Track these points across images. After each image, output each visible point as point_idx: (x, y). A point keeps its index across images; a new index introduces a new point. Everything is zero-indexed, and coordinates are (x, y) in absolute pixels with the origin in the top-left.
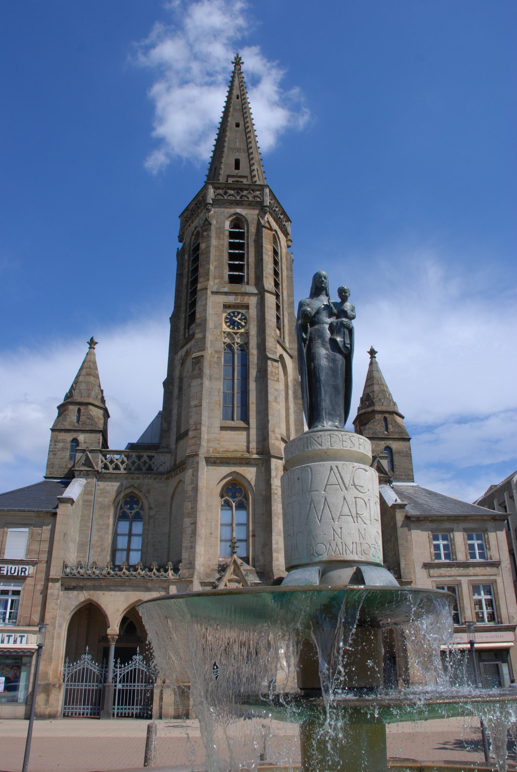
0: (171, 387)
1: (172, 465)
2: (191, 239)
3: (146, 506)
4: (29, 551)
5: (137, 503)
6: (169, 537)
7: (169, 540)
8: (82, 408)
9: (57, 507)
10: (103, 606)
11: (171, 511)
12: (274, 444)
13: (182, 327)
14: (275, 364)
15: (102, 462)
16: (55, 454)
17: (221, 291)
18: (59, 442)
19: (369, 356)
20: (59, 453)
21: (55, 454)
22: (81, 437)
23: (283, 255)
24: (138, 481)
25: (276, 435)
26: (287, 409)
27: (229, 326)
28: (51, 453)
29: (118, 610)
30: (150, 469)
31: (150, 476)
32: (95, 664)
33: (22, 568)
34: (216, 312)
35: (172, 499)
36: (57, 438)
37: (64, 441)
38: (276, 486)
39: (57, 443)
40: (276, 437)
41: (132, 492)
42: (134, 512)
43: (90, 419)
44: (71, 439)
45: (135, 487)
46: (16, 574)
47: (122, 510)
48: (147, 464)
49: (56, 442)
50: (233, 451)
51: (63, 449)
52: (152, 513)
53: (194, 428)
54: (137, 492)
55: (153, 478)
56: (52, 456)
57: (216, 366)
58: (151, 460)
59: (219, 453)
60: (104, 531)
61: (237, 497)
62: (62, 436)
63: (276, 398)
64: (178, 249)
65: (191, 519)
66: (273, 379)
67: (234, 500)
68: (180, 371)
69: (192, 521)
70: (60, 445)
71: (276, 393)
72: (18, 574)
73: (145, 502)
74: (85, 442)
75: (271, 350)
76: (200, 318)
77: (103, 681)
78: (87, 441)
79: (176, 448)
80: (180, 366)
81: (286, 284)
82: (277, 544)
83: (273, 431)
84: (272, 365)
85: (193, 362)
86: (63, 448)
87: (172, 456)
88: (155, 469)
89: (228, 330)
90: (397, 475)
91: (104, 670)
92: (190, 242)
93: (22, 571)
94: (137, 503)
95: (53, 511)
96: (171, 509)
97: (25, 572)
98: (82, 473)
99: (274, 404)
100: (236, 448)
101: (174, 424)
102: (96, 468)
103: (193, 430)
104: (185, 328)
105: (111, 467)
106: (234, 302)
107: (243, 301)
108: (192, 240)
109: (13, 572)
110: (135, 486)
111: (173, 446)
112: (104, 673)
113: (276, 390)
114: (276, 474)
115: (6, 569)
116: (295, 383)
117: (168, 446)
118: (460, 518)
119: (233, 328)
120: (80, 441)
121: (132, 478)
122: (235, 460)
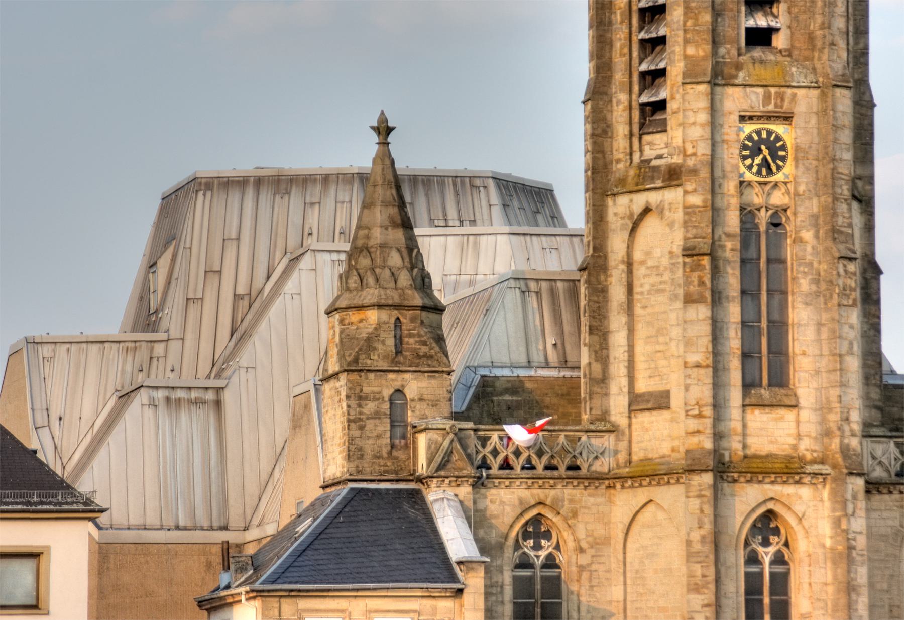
0: (602, 278)
5: (548, 535)
11: (625, 558)
18: (366, 398)
20: (370, 424)
21: (362, 428)
24: (552, 493)
28: (352, 425)
30: (574, 467)
31: (575, 482)
36: (361, 391)
37: (377, 398)
38: (854, 532)
39: (364, 403)
40: (852, 430)
41: (539, 514)
42: (543, 554)
43: (424, 343)
44: (392, 391)
47: (521, 551)
51: (377, 415)
52: (584, 560)
53: (696, 412)
56: (357, 433)
62: (372, 385)
65: (702, 597)
68: (628, 247)
69: (706, 602)
73: (567, 535)
75: (841, 232)
76: (694, 154)
78: (425, 397)
79: (630, 425)
84: (846, 271)
85: (685, 264)
94: (548, 535)
96: (625, 553)
98: (447, 481)
103: (695, 416)
105: (495, 463)
106: (762, 108)
107: (782, 107)
110: (548, 502)
114: (854, 509)
116: (866, 265)
117: (604, 416)
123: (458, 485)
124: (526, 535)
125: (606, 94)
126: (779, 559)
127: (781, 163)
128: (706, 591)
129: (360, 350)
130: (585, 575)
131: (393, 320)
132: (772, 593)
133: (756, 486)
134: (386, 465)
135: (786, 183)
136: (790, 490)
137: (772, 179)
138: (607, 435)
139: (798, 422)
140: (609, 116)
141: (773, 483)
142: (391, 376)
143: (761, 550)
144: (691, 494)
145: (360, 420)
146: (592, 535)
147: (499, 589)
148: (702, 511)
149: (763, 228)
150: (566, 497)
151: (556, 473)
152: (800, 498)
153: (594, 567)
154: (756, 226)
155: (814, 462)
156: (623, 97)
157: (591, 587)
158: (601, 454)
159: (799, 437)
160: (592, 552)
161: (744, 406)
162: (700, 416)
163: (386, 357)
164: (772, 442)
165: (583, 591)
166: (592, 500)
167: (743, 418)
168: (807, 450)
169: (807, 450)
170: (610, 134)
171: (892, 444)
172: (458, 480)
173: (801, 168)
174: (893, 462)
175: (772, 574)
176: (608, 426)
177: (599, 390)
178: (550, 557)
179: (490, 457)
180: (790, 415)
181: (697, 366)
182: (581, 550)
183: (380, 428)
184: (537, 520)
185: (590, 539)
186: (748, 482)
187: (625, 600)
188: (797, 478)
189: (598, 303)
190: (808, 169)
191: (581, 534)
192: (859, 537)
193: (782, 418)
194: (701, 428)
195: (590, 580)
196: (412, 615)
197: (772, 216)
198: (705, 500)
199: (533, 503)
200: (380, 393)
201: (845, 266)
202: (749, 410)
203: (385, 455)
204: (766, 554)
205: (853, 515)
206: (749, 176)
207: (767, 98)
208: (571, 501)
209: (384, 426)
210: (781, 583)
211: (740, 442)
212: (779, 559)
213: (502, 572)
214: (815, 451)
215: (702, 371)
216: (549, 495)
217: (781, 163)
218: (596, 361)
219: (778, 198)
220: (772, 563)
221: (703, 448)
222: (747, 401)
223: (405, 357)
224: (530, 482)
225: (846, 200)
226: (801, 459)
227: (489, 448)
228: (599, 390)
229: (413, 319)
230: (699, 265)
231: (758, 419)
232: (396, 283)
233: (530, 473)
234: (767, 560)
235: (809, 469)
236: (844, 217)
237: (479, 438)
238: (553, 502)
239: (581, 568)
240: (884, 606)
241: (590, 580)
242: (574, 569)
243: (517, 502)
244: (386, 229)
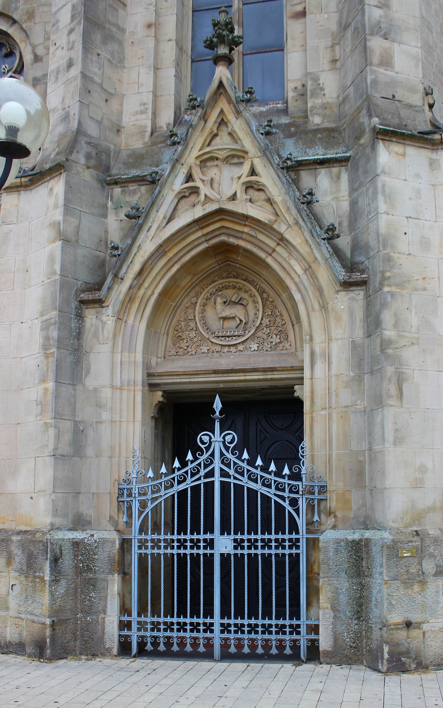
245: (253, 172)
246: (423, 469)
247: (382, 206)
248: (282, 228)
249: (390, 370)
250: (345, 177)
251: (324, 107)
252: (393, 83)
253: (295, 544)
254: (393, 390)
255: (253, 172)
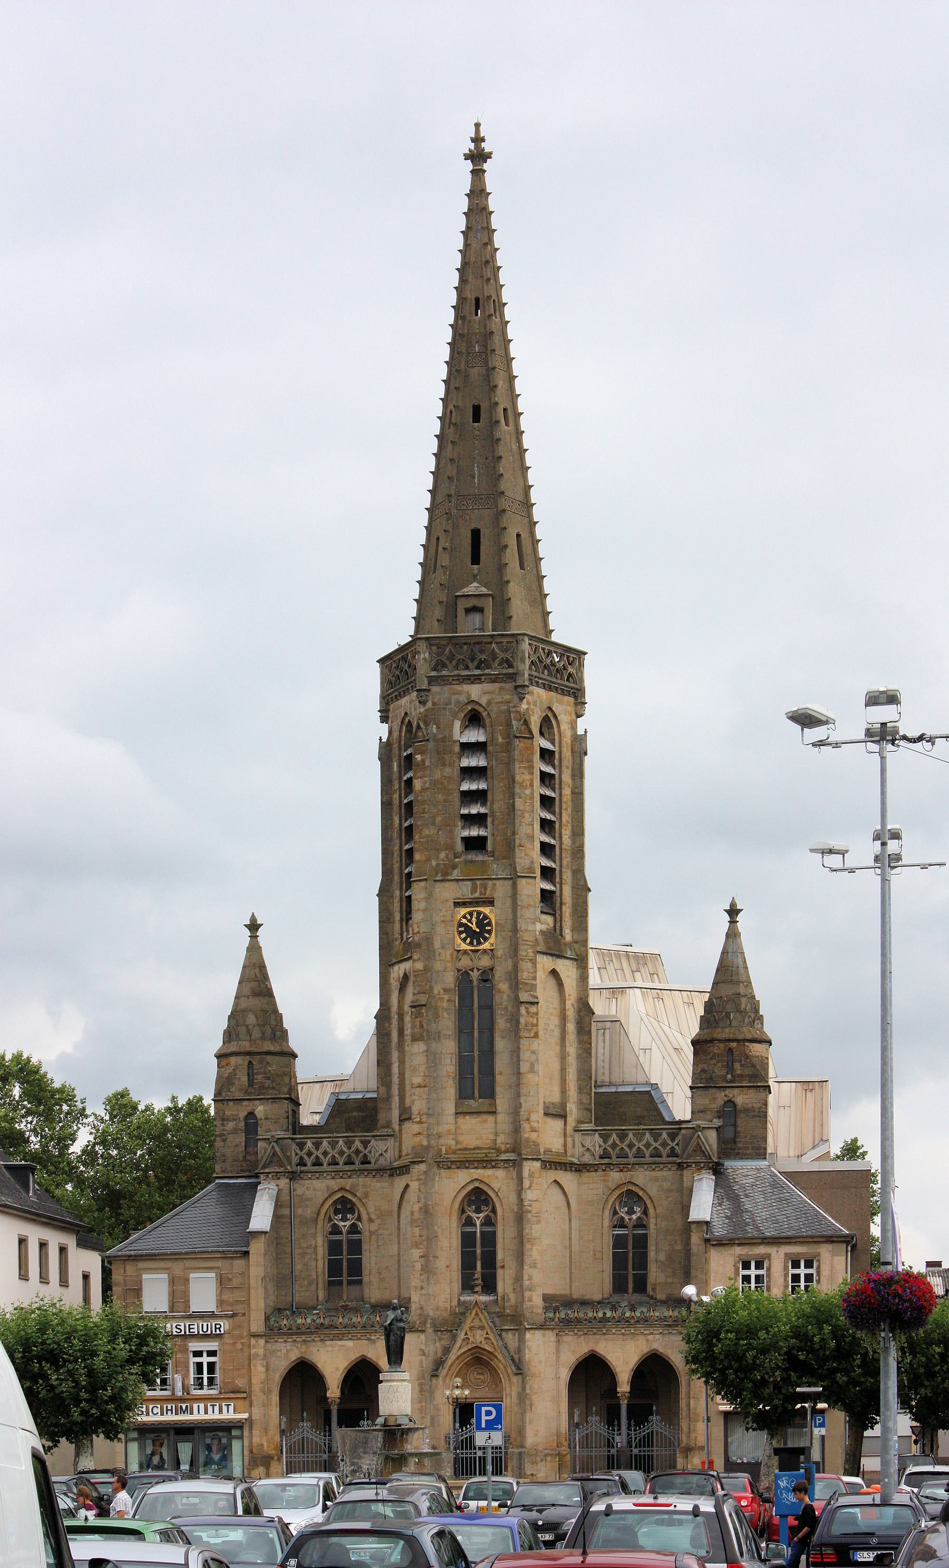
0: (387, 1025)
1: (397, 1156)
2: (400, 731)
3: (364, 1216)
4: (220, 1302)
6: (399, 1261)
7: (399, 1266)
8: (256, 1060)
9: (247, 1245)
10: (319, 1365)
11: (399, 1225)
12: (528, 1138)
13: (397, 916)
14: (533, 1009)
15: (297, 1154)
16: (224, 1141)
17: (450, 878)
18: (228, 1120)
19: (727, 918)
20: (230, 1138)
21: (224, 1141)
22: (260, 1110)
23: (564, 742)
25: (532, 1124)
26: (563, 1057)
27: (464, 940)
29: (337, 1369)
30: (366, 1161)
31: (366, 1173)
32: (316, 1432)
33: (216, 1325)
34: (442, 919)
35: (400, 1207)
36: (224, 1114)
38: (530, 1201)
40: (531, 1127)
41: (343, 1196)
42: (348, 1223)
43: (268, 1078)
44: (245, 1113)
45: (347, 1190)
46: (209, 1332)
47: (332, 1223)
48: (361, 1155)
49: (223, 1120)
50: (475, 1149)
51: (235, 1131)
52: (373, 1227)
54: (350, 1197)
55: (371, 1176)
57: (445, 1015)
58: (365, 1148)
59: (454, 1153)
60: (309, 1256)
61: (480, 1212)
63: (532, 1066)
64: (381, 739)
66: (527, 1035)
67: (478, 1215)
70: (231, 1125)
71: (533, 1058)
72: (212, 1332)
74: (266, 1119)
75: (527, 984)
77: (327, 1450)
78: (269, 1117)
79: (400, 1131)
80: (397, 991)
81: (570, 810)
82: (530, 1279)
83: (528, 1120)
84: (528, 1012)
86: (235, 1129)
87: (395, 1142)
88: (373, 1161)
89: (464, 946)
90: (740, 1149)
91: (327, 1438)
92: (400, 736)
93: (216, 1328)
95: (244, 1249)
96: (399, 1222)
97: (219, 1329)
98: (270, 1176)
99: (530, 1076)
100: (478, 1143)
101: (395, 1090)
102: (289, 1167)
104: (401, 918)
108: (403, 734)
109: (205, 1330)
110: (348, 1188)
111: (397, 1128)
112: (327, 1442)
113: (533, 1052)
114: (531, 1184)
115: (195, 1327)
117: (388, 1125)
118: (781, 1241)
119: (471, 943)
120: (259, 1116)
121: (341, 1178)
122: (476, 1163)
123: (279, 1178)
124: (337, 1212)
125: (388, 891)
126: (488, 1222)
127: (487, 936)
128: (422, 1246)
129: (223, 1085)
130: (374, 1237)
131: (246, 1063)
132: (482, 1246)
133: (464, 1170)
134: (242, 1166)
135: (492, 950)
136: (489, 1172)
137: (480, 947)
138: (389, 1138)
139: (496, 1123)
140: (391, 907)
141: (476, 1168)
142: (245, 1103)
143: (474, 1215)
144: (414, 1178)
145: (224, 1135)
146: (379, 1210)
147: (313, 1250)
148: (420, 1190)
149: (475, 983)
150: (361, 1183)
151: (352, 1167)
152: (497, 1178)
153: (381, 1231)
154: (471, 981)
155: (507, 1151)
156: (397, 893)
157: (378, 1246)
158: (385, 1152)
159: (496, 1134)
160: (378, 1221)
161: (456, 1113)
162: (420, 1122)
163: (241, 1090)
164: (477, 1139)
165: (372, 1249)
166: (379, 1185)
167: (456, 1122)
168: (502, 1143)
169: (502, 1143)
170: (392, 920)
171: (597, 1135)
172: (277, 1176)
173: (500, 939)
174: (597, 1148)
175: (482, 1233)
176: (390, 1131)
177: (384, 1106)
178: (354, 1226)
179: (305, 1157)
180: (491, 1118)
181: (419, 1087)
182: (371, 1220)
183: (238, 1140)
184: (343, 1200)
185: (378, 1212)
186: (458, 1168)
187: (399, 1254)
188: (493, 1164)
189: (383, 1043)
190: (504, 939)
191: (371, 1210)
192: (534, 1204)
193: (485, 1121)
194: (421, 1131)
195: (377, 1242)
196: (216, 1270)
197: (482, 974)
198: (422, 1182)
199: (337, 1189)
200: (236, 1115)
201: (527, 1008)
202: (461, 1117)
203: (241, 1159)
204: (478, 1218)
205: (530, 1188)
206: (464, 946)
207: (474, 890)
208: (364, 1186)
209: (241, 1138)
210: (490, 1239)
211: (453, 1139)
212: (488, 1222)
213: (315, 1238)
214: (507, 1144)
215: (422, 1090)
216: (348, 1183)
217: (487, 936)
218: (383, 1085)
219: (485, 962)
220: (482, 1225)
221: (422, 1146)
222: (459, 1111)
223: (255, 1089)
224: (333, 1174)
225: (530, 960)
226: (499, 1151)
227: (321, 1150)
228: (384, 1106)
229: (261, 1062)
230: (420, 1013)
231: (468, 1123)
232: (250, 1036)
233: (333, 1168)
234: (478, 1223)
235: (503, 1157)
236: (529, 972)
237: (298, 1144)
238: (350, 1187)
239: (371, 1233)
240: (589, 1252)
241: (377, 1242)
242: (367, 1233)
243: (325, 1189)
244: (248, 998)
245: (487, 1334)
246: (538, 1431)
247: (527, 1352)
248: (497, 1354)
249: (528, 1402)
250: (517, 1334)
251: (511, 1306)
252: (532, 1307)
253: (501, 1453)
254: (529, 1408)
255: (487, 1334)
